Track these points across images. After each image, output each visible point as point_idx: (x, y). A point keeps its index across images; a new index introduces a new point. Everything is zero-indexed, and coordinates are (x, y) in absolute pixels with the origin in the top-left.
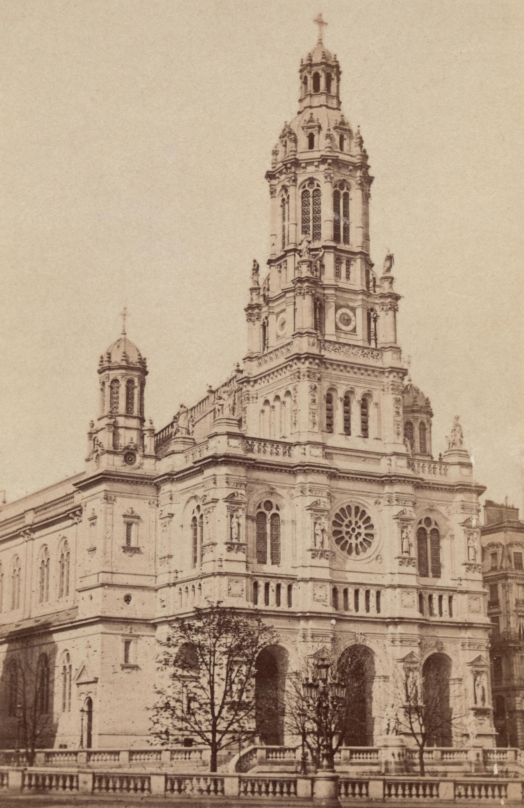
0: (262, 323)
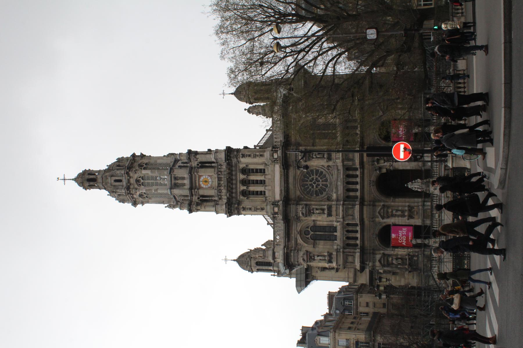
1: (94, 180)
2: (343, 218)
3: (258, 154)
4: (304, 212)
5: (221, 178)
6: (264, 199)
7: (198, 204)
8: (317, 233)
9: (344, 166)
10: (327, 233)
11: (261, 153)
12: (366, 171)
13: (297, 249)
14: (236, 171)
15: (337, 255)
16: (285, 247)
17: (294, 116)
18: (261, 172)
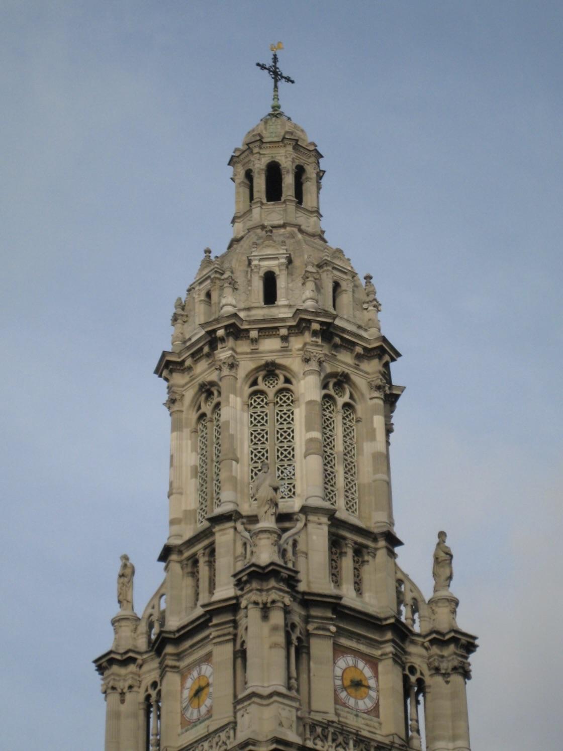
0: (141, 697)
1: (274, 193)
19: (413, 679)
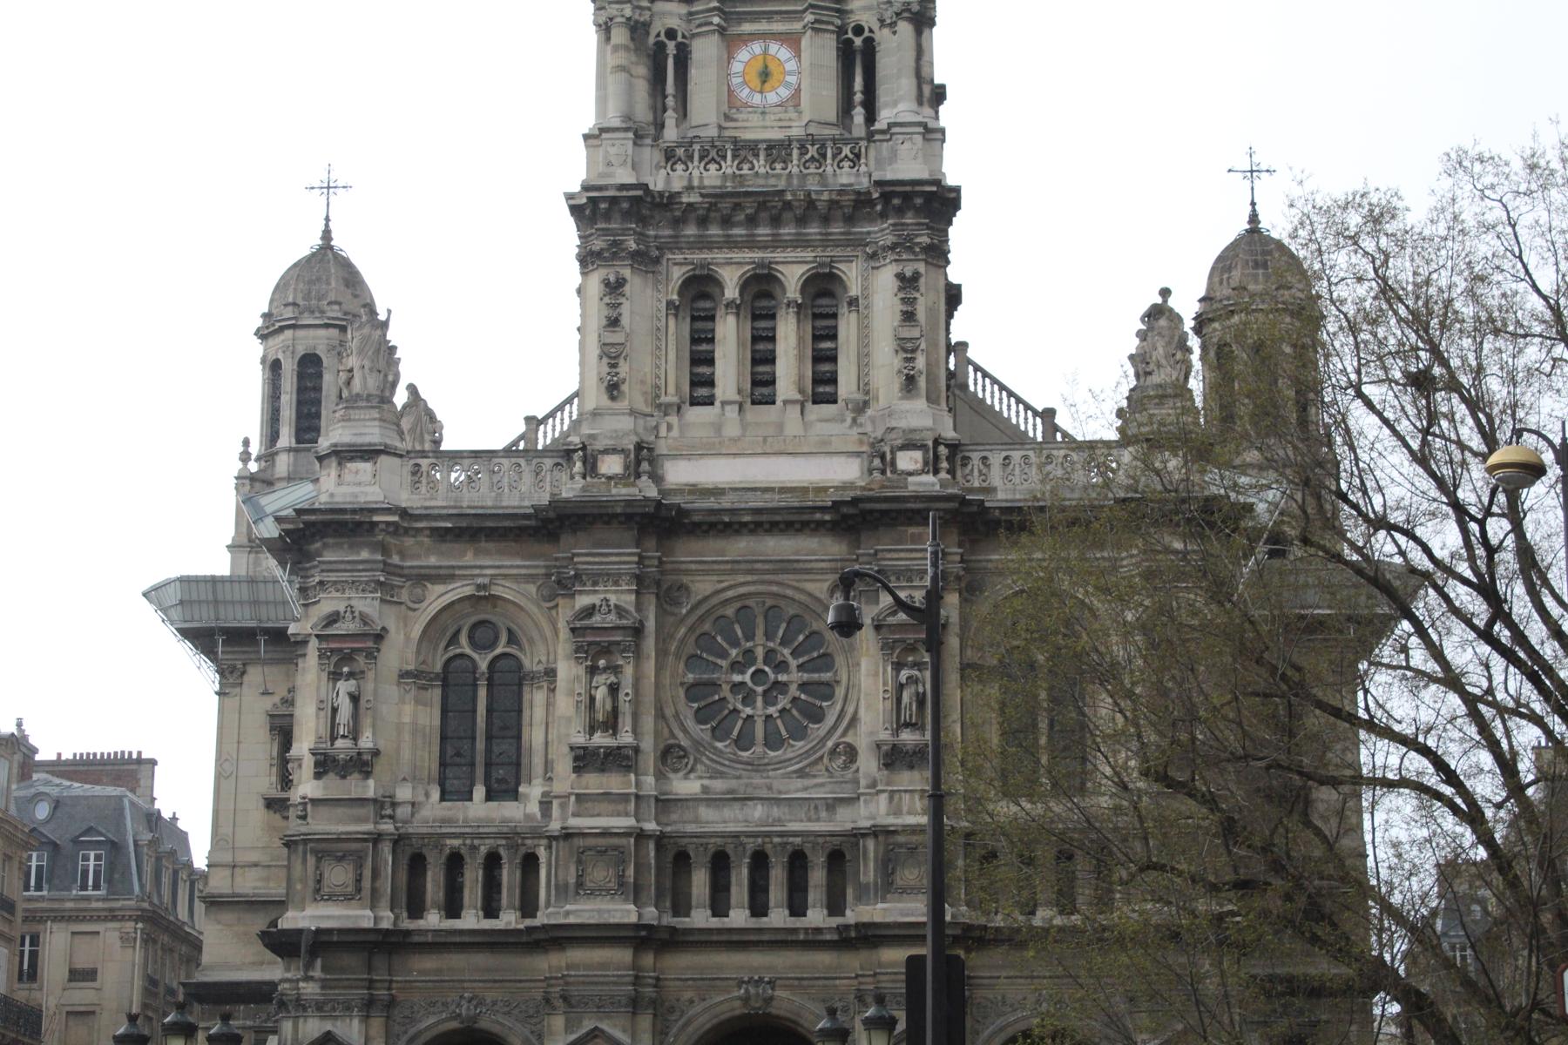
2: (567, 835)
3: (921, 362)
4: (596, 620)
5: (786, 161)
6: (671, 398)
7: (637, 29)
8: (482, 693)
9: (856, 835)
10: (480, 745)
11: (922, 382)
12: (824, 958)
13: (391, 583)
14: (825, 242)
15: (362, 801)
16: (404, 513)
17: (1130, 561)
18: (818, 380)
19: (858, 41)
